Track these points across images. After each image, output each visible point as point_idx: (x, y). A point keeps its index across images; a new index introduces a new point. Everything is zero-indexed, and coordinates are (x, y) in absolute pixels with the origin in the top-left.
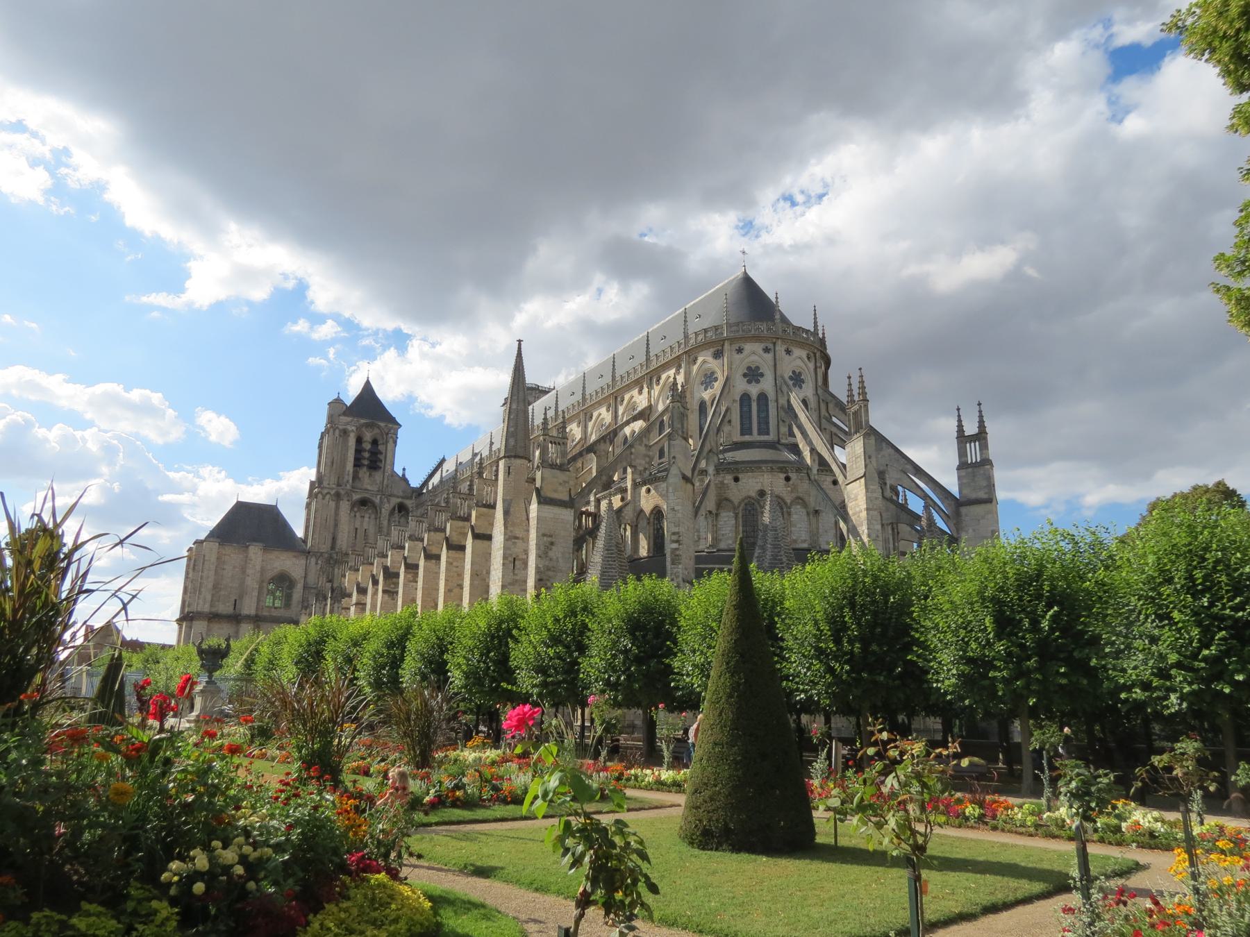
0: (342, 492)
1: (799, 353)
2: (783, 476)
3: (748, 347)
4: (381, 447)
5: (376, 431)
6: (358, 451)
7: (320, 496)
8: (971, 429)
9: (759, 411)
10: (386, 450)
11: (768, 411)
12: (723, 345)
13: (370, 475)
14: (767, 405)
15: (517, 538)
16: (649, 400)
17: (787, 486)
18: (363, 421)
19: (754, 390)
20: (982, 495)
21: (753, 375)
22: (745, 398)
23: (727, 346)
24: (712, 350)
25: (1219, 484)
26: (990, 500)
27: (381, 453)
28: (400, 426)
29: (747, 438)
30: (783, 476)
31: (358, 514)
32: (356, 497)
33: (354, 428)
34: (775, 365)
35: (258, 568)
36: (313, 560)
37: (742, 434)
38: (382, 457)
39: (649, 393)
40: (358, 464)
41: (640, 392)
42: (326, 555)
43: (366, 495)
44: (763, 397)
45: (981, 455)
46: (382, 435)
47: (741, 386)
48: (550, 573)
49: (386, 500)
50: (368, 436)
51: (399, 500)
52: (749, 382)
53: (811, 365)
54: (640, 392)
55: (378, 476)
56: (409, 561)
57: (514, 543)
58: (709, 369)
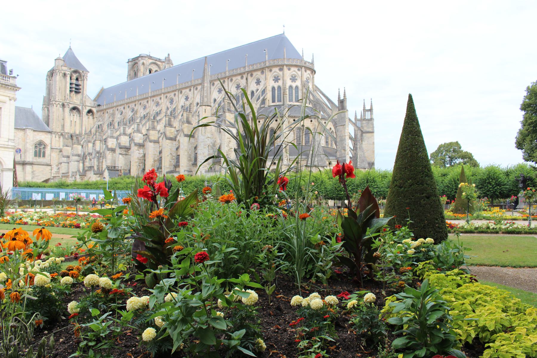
0: (66, 104)
1: (309, 72)
2: (310, 120)
3: (293, 69)
4: (80, 82)
5: (77, 74)
6: (71, 84)
7: (55, 105)
8: (367, 107)
9: (295, 93)
10: (84, 83)
11: (298, 93)
12: (283, 67)
13: (76, 96)
14: (298, 92)
15: (209, 138)
16: (247, 83)
17: (311, 124)
18: (72, 70)
19: (294, 85)
20: (370, 130)
21: (293, 79)
22: (291, 87)
23: (285, 67)
24: (278, 68)
25: (457, 143)
26: (373, 132)
27: (80, 85)
28: (89, 72)
29: (291, 103)
30: (310, 120)
31: (71, 114)
32: (71, 106)
33: (69, 73)
34: (302, 76)
35: (31, 139)
36: (54, 135)
37: (289, 101)
38: (80, 87)
39: (247, 79)
40: (71, 91)
41: (242, 78)
42: (59, 134)
43: (75, 105)
44: (297, 87)
45: (371, 116)
46: (81, 76)
47: (289, 83)
48: (230, 152)
49: (84, 108)
50: (75, 76)
51: (90, 108)
52: (292, 82)
53: (312, 76)
54: (242, 78)
55: (79, 96)
56: (135, 142)
57: (208, 140)
58: (276, 75)
